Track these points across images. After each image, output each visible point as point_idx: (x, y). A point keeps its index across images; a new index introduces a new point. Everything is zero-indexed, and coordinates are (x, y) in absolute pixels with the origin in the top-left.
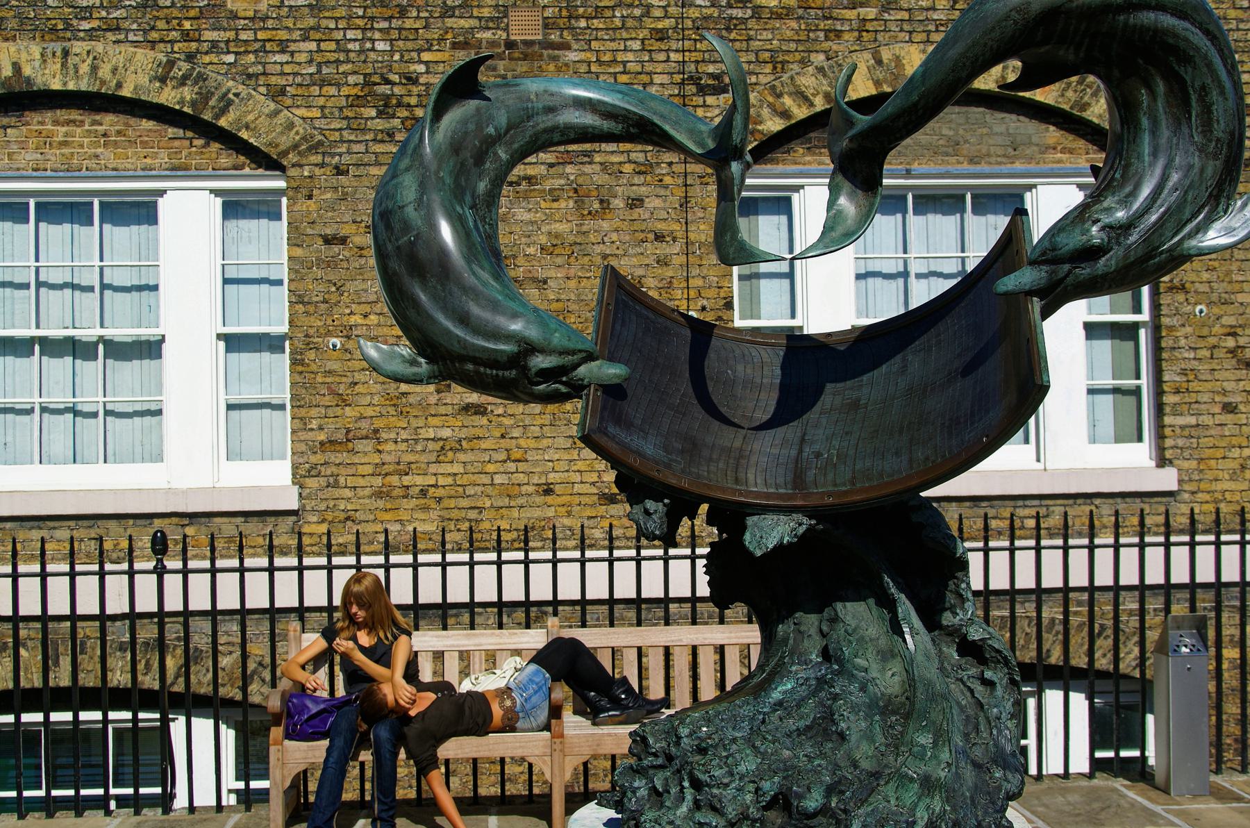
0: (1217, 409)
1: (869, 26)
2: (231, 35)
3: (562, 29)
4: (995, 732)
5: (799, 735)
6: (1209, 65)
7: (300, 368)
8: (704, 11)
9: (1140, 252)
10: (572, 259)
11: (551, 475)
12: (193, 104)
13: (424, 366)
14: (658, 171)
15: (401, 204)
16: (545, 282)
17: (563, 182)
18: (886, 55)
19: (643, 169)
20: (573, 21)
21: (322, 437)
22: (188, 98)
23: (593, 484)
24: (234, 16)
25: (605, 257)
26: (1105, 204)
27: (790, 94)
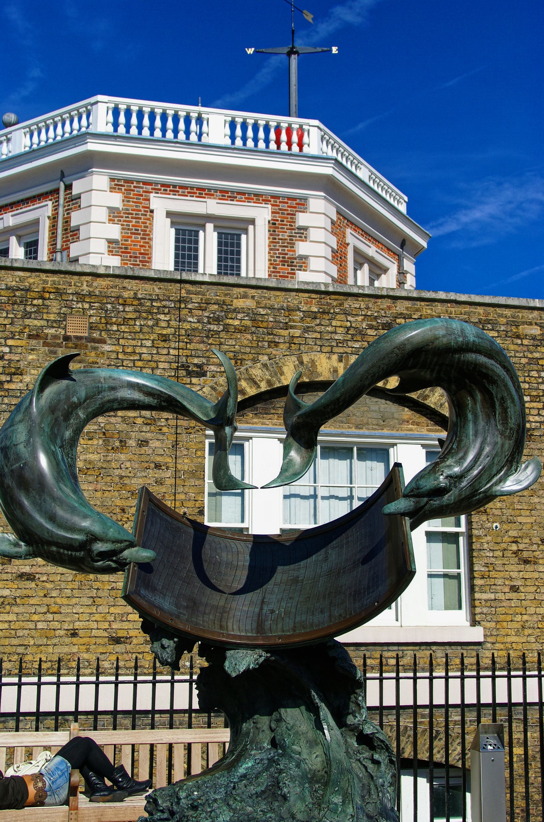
0: (507, 589)
3: (101, 331)
4: (380, 795)
5: (257, 797)
6: (506, 386)
8: (193, 325)
9: (468, 493)
10: (100, 478)
11: (77, 624)
13: (23, 547)
14: (159, 424)
15: (15, 443)
17: (96, 427)
18: (306, 359)
19: (149, 422)
20: (108, 326)
23: (105, 630)
25: (121, 477)
26: (448, 463)
27: (245, 380)
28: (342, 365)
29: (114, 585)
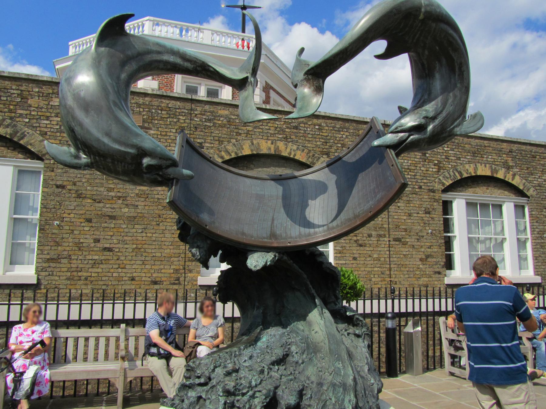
0: (351, 259)
1: (250, 133)
2: (28, 112)
7: (42, 232)
12: (11, 135)
16: (137, 206)
18: (255, 142)
21: (48, 257)
22: (9, 132)
23: (149, 277)
24: (30, 106)
25: (158, 199)
27: (224, 151)
28: (273, 146)
29: (154, 254)
